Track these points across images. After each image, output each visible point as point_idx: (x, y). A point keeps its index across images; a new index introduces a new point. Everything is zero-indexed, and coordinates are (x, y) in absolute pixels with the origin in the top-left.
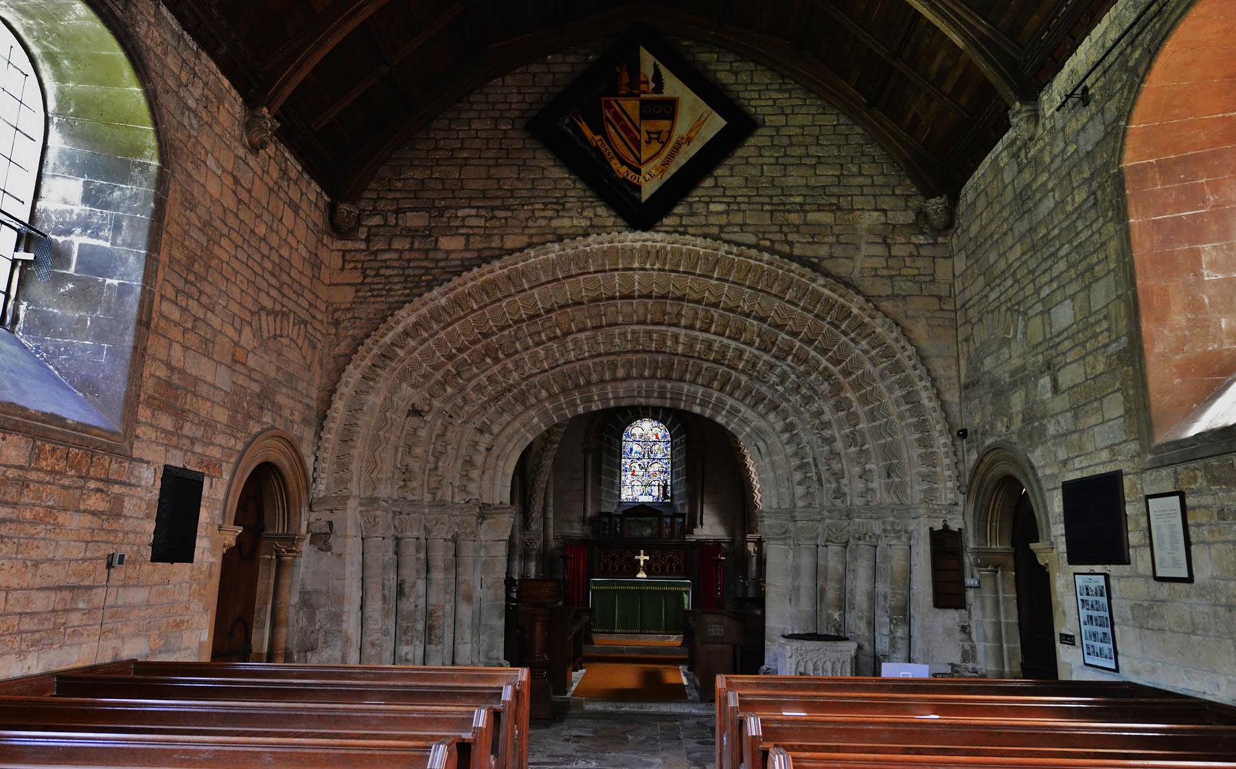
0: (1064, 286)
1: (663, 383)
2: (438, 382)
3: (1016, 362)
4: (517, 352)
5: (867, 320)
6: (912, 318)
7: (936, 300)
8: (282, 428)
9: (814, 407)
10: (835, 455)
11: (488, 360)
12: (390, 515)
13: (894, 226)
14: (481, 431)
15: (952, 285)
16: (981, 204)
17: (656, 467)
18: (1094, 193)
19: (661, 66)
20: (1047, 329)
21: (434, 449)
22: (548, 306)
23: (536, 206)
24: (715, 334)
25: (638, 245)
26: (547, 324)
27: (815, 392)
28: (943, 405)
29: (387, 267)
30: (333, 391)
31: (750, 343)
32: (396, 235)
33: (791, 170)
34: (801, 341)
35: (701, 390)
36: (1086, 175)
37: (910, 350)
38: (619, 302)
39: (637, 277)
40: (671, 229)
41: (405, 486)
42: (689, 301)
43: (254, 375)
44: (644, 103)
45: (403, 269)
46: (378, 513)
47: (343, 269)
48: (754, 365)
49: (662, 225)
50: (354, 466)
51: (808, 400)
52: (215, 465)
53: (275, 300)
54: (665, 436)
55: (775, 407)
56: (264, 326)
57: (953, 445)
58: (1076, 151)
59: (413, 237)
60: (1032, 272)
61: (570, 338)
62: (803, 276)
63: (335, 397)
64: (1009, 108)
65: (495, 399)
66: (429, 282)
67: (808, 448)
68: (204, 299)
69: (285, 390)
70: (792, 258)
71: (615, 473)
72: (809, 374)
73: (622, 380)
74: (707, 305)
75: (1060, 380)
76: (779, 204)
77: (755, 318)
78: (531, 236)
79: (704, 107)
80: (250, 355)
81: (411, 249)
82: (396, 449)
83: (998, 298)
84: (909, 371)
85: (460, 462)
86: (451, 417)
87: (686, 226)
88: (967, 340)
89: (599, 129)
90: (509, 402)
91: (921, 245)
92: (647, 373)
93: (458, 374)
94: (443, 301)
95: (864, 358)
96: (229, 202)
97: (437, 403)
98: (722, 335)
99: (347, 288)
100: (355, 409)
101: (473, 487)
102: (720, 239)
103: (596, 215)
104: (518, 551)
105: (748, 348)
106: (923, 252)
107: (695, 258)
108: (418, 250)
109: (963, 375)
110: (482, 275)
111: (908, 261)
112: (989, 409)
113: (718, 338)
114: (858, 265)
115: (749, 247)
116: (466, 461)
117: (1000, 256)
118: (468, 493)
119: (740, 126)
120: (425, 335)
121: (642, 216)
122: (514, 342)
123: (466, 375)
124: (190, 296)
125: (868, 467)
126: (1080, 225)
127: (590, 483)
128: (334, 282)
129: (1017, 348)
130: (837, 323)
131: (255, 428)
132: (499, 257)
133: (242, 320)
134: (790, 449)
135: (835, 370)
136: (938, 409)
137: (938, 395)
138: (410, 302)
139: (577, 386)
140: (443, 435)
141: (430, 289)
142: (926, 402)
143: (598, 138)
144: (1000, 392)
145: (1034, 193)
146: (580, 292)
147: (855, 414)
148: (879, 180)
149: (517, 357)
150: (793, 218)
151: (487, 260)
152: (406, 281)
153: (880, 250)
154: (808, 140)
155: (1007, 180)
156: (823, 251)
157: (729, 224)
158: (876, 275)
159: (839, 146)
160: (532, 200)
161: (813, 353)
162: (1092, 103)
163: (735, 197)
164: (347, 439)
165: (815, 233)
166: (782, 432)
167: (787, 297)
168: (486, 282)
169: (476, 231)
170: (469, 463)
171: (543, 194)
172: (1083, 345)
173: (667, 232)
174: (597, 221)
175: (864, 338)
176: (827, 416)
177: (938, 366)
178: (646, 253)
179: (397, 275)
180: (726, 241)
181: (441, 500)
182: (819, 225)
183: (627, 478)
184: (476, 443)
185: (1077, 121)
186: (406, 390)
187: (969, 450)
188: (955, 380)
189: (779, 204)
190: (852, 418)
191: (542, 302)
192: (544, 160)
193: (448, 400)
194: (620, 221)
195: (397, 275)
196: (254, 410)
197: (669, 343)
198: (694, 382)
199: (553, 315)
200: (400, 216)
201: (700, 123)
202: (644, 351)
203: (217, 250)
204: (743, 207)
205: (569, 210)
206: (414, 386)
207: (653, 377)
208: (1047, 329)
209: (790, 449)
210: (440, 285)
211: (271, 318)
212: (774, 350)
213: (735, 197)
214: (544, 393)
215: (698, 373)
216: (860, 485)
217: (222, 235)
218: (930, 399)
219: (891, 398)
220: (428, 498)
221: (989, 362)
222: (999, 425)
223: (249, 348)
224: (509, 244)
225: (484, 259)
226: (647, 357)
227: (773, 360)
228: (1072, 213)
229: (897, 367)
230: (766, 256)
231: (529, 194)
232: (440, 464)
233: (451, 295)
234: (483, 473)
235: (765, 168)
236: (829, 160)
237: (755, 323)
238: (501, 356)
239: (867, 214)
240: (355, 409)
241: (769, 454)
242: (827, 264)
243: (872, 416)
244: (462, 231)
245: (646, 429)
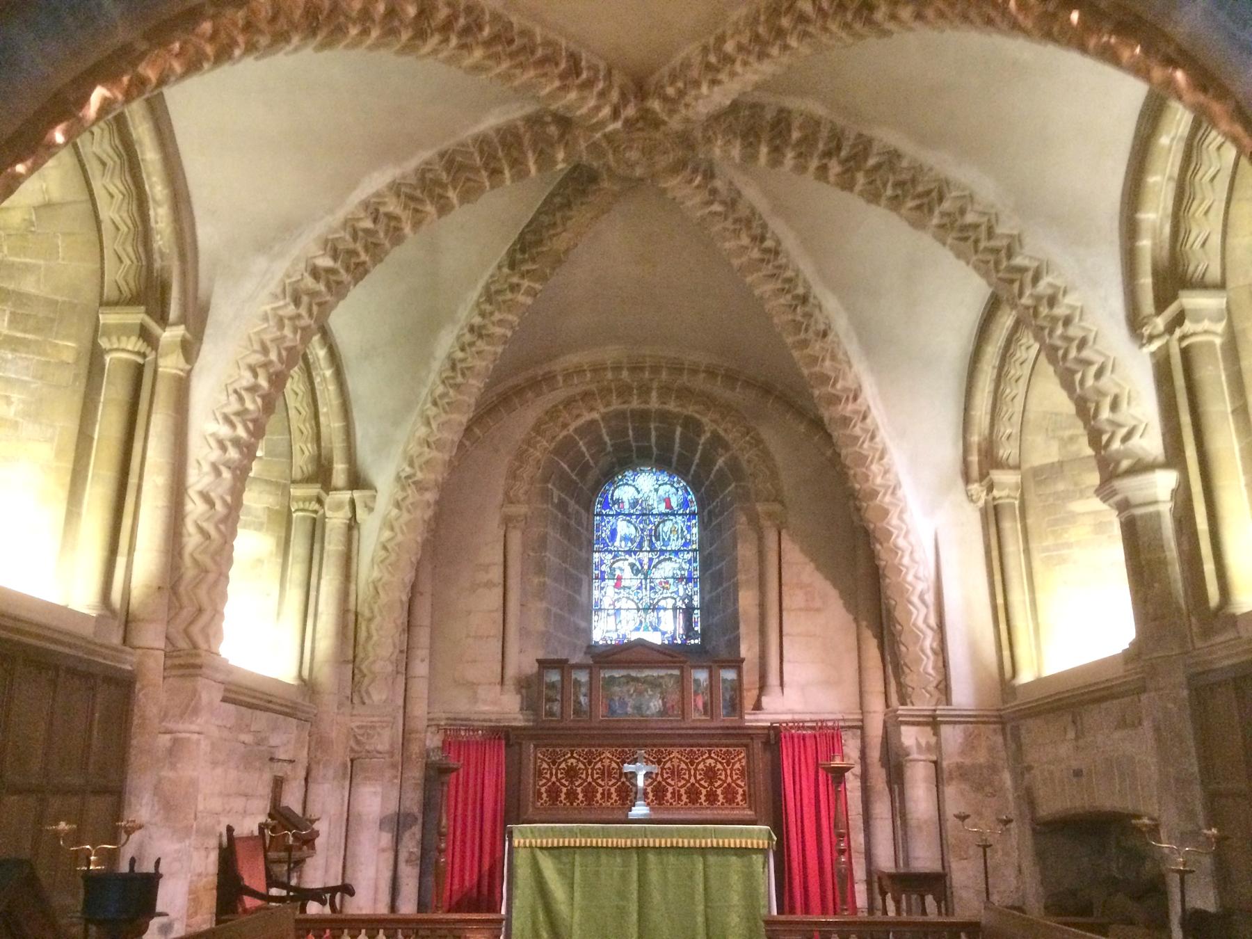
17: (667, 569)
54: (685, 504)
71: (579, 582)
104: (340, 754)
183: (605, 594)
245: (646, 487)
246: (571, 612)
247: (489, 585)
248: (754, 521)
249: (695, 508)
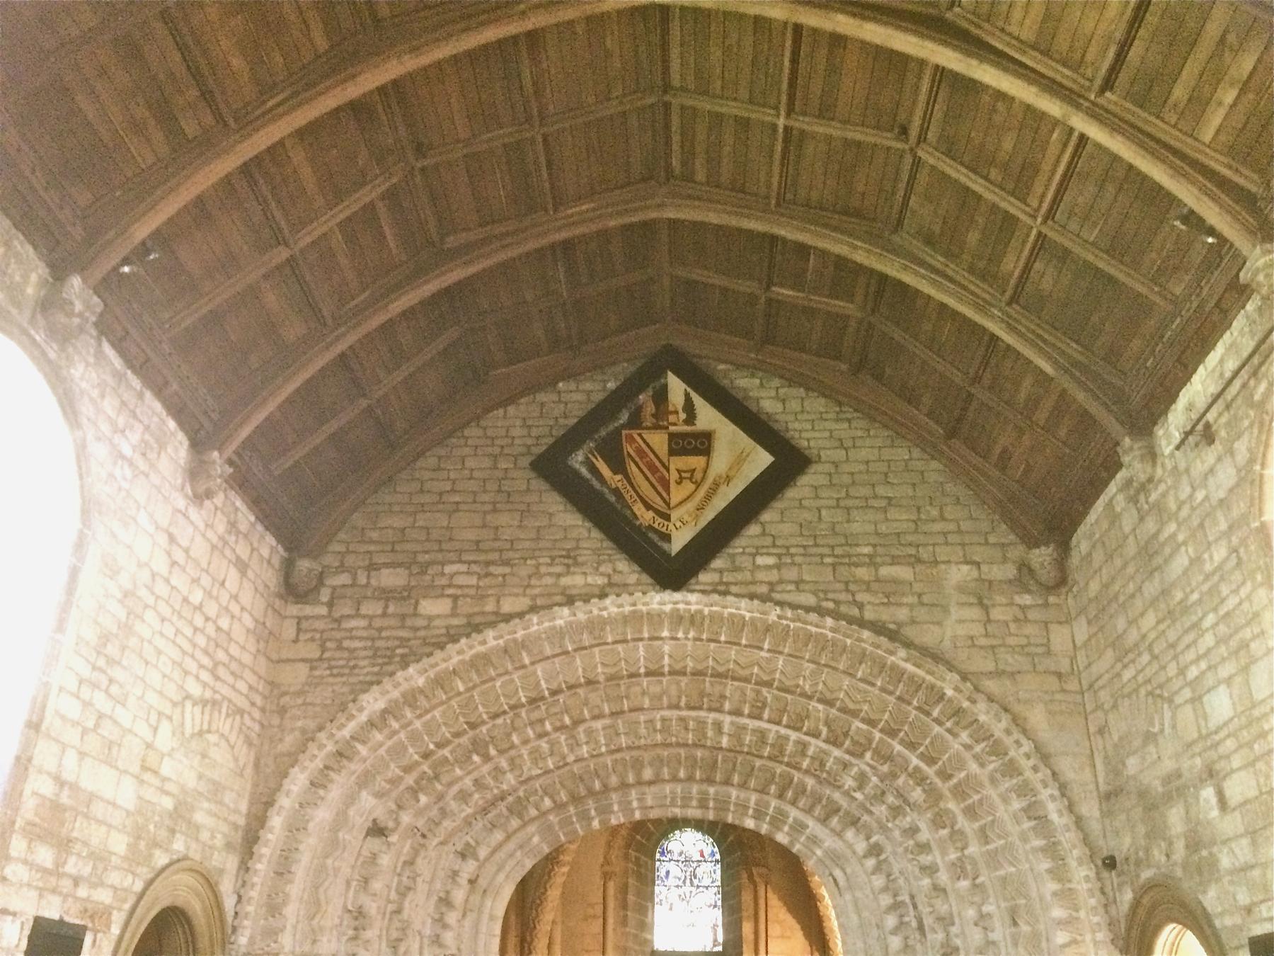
0: (1215, 667)
1: (704, 787)
2: (409, 788)
3: (1168, 765)
4: (513, 747)
5: (966, 704)
6: (1026, 702)
7: (1053, 680)
8: (197, 857)
9: (906, 821)
10: (938, 889)
11: (476, 758)
13: (990, 582)
14: (463, 856)
15: (1073, 659)
16: (1098, 557)
18: (1236, 551)
19: (694, 395)
20: (1203, 723)
21: (399, 883)
22: (554, 686)
23: (541, 560)
24: (769, 721)
25: (668, 608)
26: (553, 710)
27: (906, 801)
28: (1079, 822)
29: (351, 638)
30: (269, 804)
31: (816, 735)
32: (365, 597)
33: (854, 513)
34: (881, 731)
35: (754, 797)
36: (1223, 526)
37: (1027, 746)
38: (645, 681)
39: (666, 649)
40: (707, 588)
42: (734, 679)
43: (169, 787)
44: (672, 436)
45: (373, 640)
47: (296, 641)
48: (822, 764)
49: (697, 583)
50: (291, 911)
51: (896, 812)
52: (100, 915)
53: (205, 685)
54: (713, 854)
55: (854, 822)
56: (188, 716)
57: (1099, 879)
58: (1207, 498)
59: (387, 600)
60: (1172, 646)
61: (581, 729)
62: (878, 647)
63: (272, 812)
64: (1117, 444)
65: (485, 811)
66: (403, 656)
67: (901, 881)
68: (114, 689)
69: (206, 805)
70: (862, 623)
71: (647, 908)
72: (894, 776)
73: (650, 783)
74: (757, 683)
75: (1228, 793)
76: (843, 556)
77: (820, 701)
78: (534, 598)
79: (745, 440)
80: (166, 758)
81: (384, 615)
82: (348, 883)
83: (1135, 677)
84: (1028, 774)
86: (424, 836)
87: (727, 584)
88: (1101, 732)
89: (618, 465)
90: (500, 815)
91: (1029, 607)
92: (682, 774)
93: (437, 777)
94: (421, 681)
95: (967, 755)
96: (161, 565)
97: (406, 818)
98: (778, 723)
99: (301, 665)
100: (296, 828)
102: (771, 600)
103: (614, 570)
105: (813, 741)
106: (1032, 615)
107: (738, 625)
108: (393, 615)
109: (1101, 780)
110: (471, 647)
111: (1013, 626)
112: (1141, 830)
113: (775, 728)
114: (949, 633)
115: (808, 609)
116: (440, 899)
117: (1130, 623)
119: (790, 462)
120: (395, 725)
121: (673, 572)
122: (509, 735)
123: (445, 779)
124: (95, 686)
125: (985, 909)
126: (1225, 590)
127: (611, 921)
128: (284, 657)
129: (1168, 747)
130: (927, 708)
131: (161, 859)
132: (492, 625)
133: (160, 714)
134: (879, 881)
135: (930, 771)
136: (1073, 827)
137: (1071, 808)
138: (379, 683)
139: (591, 793)
141: (405, 666)
142: (1054, 817)
143: (619, 477)
144: (1152, 805)
145: (1163, 545)
146: (596, 667)
147: (961, 832)
148: (965, 526)
149: (513, 753)
150: (862, 573)
151: (477, 628)
152: (375, 656)
153: (975, 613)
154: (875, 478)
155: (1127, 529)
156: (902, 614)
157: (781, 582)
158: (974, 646)
159: (914, 485)
160: (537, 553)
161: (898, 748)
162: (1217, 442)
163: (788, 548)
164: (283, 871)
165: (891, 592)
166: (865, 857)
167: (860, 674)
168: (477, 656)
169: (466, 591)
170: (446, 901)
171: (549, 545)
172: (1250, 744)
173: (703, 592)
174: (616, 579)
175: (965, 728)
176: (925, 835)
177: (1066, 766)
178: (677, 619)
179: (365, 648)
180: (780, 604)
182: (895, 581)
184: (455, 874)
185: (1203, 462)
186: (367, 800)
187: (1120, 885)
188: (1092, 787)
189: (843, 556)
190: (957, 836)
191: (547, 681)
192: (554, 502)
193: (419, 813)
194: (646, 578)
195: (365, 648)
196: (163, 833)
197: (710, 733)
198: (743, 785)
199: (561, 698)
200: (373, 573)
201: (740, 459)
202: (678, 745)
203: (139, 627)
204: (798, 559)
205: (583, 564)
206: (379, 795)
207: (690, 778)
208: (1203, 723)
209: (879, 881)
210: (418, 661)
211: (198, 709)
212: (848, 743)
213: (788, 548)
214: (547, 803)
215: (749, 775)
216: (976, 936)
217: (146, 606)
218: (1061, 814)
219: (1007, 810)
221: (1132, 764)
222: (1156, 852)
223: (165, 750)
224: (507, 606)
225: (474, 628)
226: (682, 751)
227: (847, 757)
228: (1213, 573)
229: (1011, 769)
230: (829, 621)
231: (533, 545)
232: (407, 905)
233: (432, 674)
234: (464, 915)
235: (824, 512)
236: (904, 502)
237: (820, 707)
238: (493, 752)
239: (954, 568)
240: (296, 828)
241: (850, 888)
242: (909, 632)
243: (984, 836)
244: (450, 591)
246: (642, 931)
247: (595, 917)
248: (751, 877)
249: (718, 857)
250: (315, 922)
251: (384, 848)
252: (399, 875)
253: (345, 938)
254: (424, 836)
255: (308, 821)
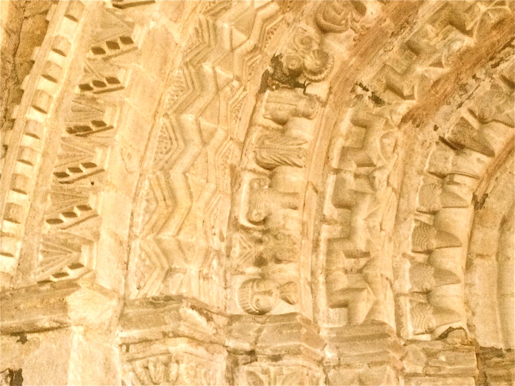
12: (221, 362)
14: (457, 146)
21: (340, 184)
41: (263, 277)
46: (180, 346)
85: (409, 227)
101: (451, 295)
116: (423, 226)
118: (439, 310)
140: (363, 144)
170: (434, 225)
181: (371, 321)
220: (329, 321)
232: (360, 220)
250: (167, 236)
251: (302, 105)
252: (337, 171)
253: (240, 280)
254: (377, 100)
255: (131, 25)
